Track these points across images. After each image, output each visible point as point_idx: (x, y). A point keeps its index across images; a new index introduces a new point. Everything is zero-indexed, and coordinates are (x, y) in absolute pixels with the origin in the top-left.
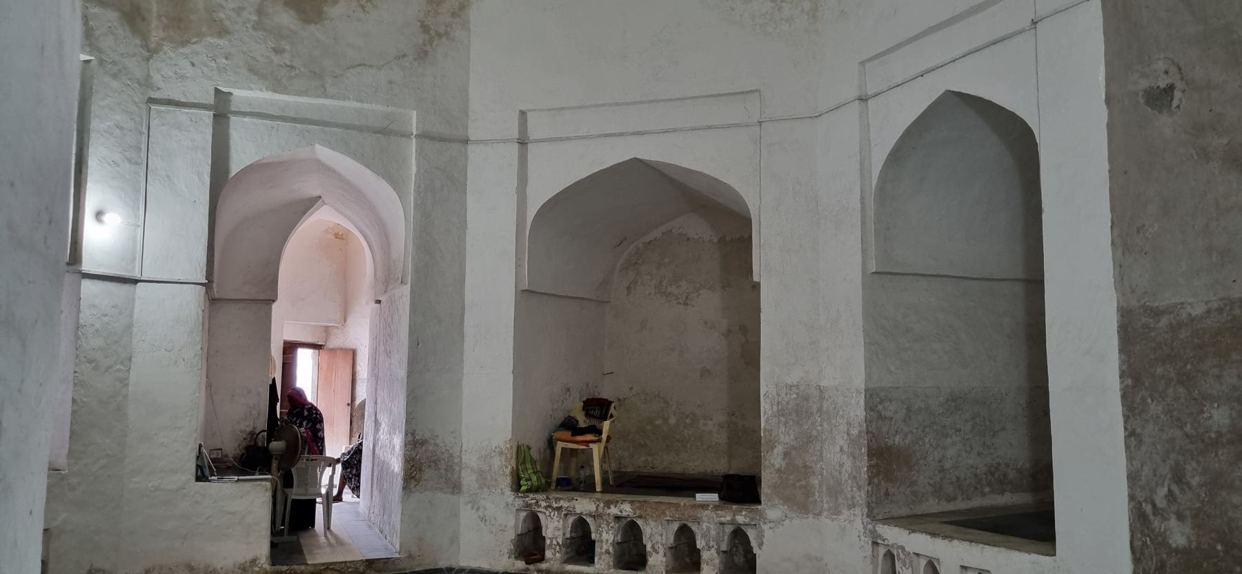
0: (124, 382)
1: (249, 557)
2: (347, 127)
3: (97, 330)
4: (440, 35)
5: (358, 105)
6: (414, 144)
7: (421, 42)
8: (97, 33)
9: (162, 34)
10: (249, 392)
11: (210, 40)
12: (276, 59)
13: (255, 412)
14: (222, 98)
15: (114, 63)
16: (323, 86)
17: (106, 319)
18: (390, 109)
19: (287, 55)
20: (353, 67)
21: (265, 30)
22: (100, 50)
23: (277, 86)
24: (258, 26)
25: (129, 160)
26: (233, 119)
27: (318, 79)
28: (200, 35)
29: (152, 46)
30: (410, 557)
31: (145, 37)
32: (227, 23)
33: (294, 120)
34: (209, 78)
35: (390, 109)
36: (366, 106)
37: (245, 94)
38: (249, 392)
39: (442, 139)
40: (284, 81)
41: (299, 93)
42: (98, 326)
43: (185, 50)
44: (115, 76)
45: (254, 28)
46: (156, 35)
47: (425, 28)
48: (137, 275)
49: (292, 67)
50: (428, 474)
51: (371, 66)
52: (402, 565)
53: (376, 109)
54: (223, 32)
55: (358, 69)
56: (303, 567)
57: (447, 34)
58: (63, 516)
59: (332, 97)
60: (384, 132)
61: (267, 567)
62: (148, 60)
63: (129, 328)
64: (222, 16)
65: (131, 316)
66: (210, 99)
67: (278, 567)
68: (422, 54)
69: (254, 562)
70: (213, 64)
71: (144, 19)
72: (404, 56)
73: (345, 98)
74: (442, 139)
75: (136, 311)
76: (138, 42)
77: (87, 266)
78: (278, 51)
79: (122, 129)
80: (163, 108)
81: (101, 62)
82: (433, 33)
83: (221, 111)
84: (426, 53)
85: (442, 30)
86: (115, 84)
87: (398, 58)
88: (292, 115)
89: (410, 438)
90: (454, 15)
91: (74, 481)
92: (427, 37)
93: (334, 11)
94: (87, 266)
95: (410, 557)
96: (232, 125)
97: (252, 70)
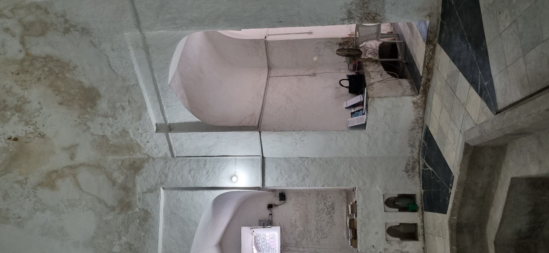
0: (313, 160)
1: (412, 105)
2: (152, 70)
3: (289, 177)
4: (66, 21)
5: (136, 67)
6: (149, 34)
7: (77, 33)
8: (149, 187)
9: (138, 154)
10: (317, 48)
11: (132, 136)
12: (128, 109)
13: (329, 44)
14: (159, 128)
15: (160, 177)
16: (133, 86)
17: (283, 172)
18: (130, 48)
19: (123, 104)
20: (114, 71)
21: (115, 114)
22: (157, 185)
23: (143, 107)
24: (114, 117)
25: (205, 165)
26: (169, 121)
27: (129, 89)
28: (132, 140)
29: (146, 157)
30: (430, 16)
31: (143, 161)
32: (120, 130)
33: (158, 96)
34: (152, 136)
35: (130, 48)
36: (134, 62)
37: (153, 117)
38: (317, 48)
39: (136, 15)
40: (139, 105)
41: (142, 97)
42: (287, 177)
43: (142, 145)
44: (167, 176)
45: (116, 119)
46: (139, 155)
47: (67, 31)
48: (260, 158)
49: (129, 101)
50: (372, 8)
51: (108, 61)
52: (435, 21)
53: (133, 56)
54: (125, 132)
55: (114, 68)
56: (423, 79)
57: (62, 16)
58: (378, 188)
59: (137, 80)
60: (146, 48)
61: (419, 97)
62: (153, 159)
63: (286, 160)
64: (116, 132)
65: (280, 159)
66: (162, 135)
67: (420, 91)
68: (85, 31)
69: (414, 103)
70: (144, 134)
71: (135, 162)
72: (92, 42)
73: (134, 75)
74: (136, 15)
75: (278, 156)
76: (147, 164)
77: (259, 185)
78: (123, 109)
79: (190, 170)
80: (175, 152)
81: (162, 184)
82: (67, 26)
83: (168, 128)
84: (83, 29)
85: (62, 20)
86: (170, 175)
87: (95, 46)
88: (156, 97)
89: (346, 21)
90: (47, 12)
91: (361, 183)
92: (72, 29)
93: (86, 83)
94: (259, 185)
95: (430, 16)
96: (173, 122)
97: (140, 119)
